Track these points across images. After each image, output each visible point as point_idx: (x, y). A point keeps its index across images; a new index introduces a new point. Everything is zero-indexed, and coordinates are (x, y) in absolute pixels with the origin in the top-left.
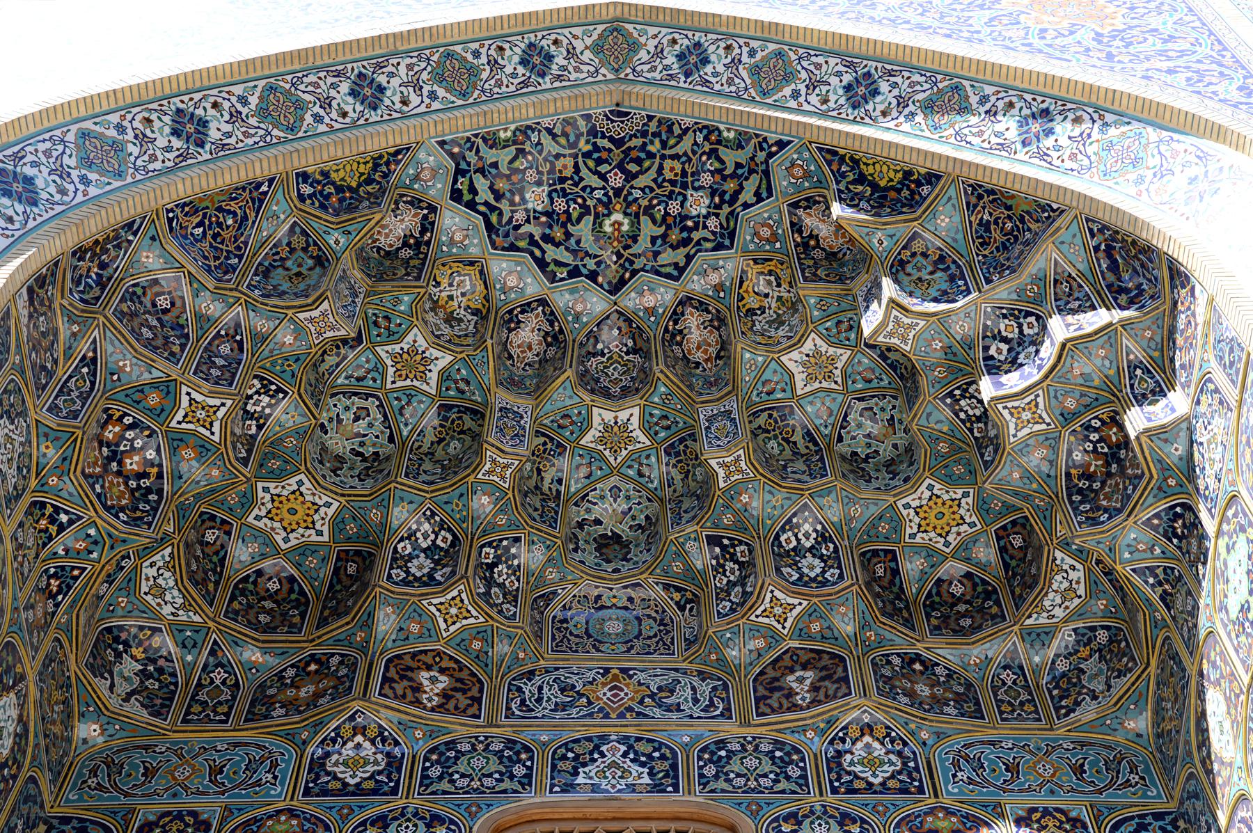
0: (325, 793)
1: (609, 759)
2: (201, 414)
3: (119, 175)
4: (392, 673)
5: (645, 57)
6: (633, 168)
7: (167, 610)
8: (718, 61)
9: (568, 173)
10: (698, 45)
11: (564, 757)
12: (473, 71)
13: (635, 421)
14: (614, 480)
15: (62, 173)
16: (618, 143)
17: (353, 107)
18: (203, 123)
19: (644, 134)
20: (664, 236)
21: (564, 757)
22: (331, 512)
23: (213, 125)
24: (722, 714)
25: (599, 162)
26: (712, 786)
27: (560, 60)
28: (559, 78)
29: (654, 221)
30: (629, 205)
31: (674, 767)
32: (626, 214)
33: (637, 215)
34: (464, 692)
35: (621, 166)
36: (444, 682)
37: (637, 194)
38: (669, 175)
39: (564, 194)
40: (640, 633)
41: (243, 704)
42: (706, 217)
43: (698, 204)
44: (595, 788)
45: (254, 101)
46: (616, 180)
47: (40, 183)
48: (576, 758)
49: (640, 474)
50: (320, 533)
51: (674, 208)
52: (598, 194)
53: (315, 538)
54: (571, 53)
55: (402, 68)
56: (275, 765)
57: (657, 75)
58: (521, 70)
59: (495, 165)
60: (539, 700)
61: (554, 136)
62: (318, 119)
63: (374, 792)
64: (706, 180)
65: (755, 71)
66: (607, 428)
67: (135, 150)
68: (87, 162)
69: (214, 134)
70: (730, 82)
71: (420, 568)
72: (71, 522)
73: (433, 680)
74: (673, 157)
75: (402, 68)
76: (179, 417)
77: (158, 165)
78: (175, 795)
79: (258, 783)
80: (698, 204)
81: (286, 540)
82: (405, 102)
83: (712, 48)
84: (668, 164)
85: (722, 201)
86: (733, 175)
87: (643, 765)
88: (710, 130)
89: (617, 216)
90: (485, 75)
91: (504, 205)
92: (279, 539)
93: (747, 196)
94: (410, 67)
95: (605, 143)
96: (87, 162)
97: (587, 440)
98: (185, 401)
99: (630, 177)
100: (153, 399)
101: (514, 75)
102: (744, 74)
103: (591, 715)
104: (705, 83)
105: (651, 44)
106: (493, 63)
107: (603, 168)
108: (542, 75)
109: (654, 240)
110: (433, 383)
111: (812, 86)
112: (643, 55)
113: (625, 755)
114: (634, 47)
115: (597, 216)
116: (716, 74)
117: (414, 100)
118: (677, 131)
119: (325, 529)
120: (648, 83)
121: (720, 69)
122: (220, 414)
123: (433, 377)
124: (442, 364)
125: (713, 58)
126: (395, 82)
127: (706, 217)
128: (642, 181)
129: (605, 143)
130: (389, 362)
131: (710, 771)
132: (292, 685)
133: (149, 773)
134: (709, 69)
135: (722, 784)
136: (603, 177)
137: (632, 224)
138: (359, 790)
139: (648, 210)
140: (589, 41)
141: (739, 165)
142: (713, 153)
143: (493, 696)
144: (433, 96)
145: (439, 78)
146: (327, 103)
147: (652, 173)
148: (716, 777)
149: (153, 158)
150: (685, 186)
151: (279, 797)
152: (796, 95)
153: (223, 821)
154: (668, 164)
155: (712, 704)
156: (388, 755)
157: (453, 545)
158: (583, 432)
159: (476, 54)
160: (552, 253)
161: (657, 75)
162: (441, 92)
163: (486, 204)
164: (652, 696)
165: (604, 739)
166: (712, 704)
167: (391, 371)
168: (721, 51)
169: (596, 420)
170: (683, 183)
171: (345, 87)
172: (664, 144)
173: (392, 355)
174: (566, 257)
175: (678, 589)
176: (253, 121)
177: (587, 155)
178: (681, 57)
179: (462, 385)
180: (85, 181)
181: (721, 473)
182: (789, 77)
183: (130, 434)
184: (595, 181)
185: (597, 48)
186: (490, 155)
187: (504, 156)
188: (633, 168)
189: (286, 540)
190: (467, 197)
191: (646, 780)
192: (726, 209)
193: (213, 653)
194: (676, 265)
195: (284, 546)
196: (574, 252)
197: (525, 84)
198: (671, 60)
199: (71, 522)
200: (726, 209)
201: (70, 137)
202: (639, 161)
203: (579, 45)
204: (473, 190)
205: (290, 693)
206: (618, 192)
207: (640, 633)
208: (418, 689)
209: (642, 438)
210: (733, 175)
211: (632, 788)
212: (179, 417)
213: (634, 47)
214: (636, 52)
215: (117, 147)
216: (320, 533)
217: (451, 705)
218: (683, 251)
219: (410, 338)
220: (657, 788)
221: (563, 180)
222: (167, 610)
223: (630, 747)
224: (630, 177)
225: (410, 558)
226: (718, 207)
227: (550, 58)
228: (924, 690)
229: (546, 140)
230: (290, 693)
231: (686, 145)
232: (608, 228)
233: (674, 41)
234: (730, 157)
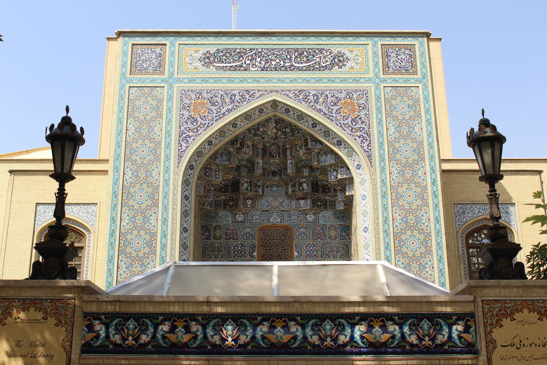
12: (251, 116)
41: (222, 204)
43: (288, 130)
51: (284, 130)
63: (243, 222)
65: (298, 116)
80: (288, 130)
93: (296, 132)
111: (307, 122)
114: (277, 106)
133: (213, 217)
138: (241, 222)
139: (280, 130)
143: (258, 204)
145: (245, 119)
152: (304, 122)
160: (264, 136)
165: (274, 212)
182: (303, 119)
185: (271, 106)
224: (277, 125)
227: (263, 110)
228: (319, 203)
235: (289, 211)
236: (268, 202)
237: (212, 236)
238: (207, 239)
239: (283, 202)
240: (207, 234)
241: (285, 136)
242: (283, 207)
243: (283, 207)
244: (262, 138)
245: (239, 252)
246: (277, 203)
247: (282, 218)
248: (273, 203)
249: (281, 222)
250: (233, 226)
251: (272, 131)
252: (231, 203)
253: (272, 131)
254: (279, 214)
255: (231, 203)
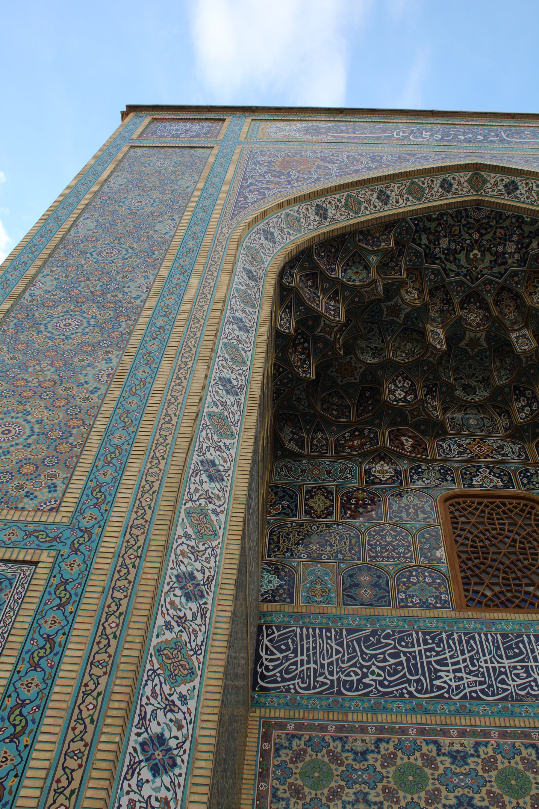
0: (374, 483)
1: (484, 475)
2: (328, 329)
3: (299, 231)
4: (392, 437)
5: (490, 186)
6: (483, 231)
7: (301, 408)
8: (522, 189)
9: (456, 233)
10: (513, 182)
11: (465, 473)
13: (483, 337)
14: (470, 361)
15: (281, 230)
16: (477, 221)
17: (378, 204)
18: (326, 210)
19: (488, 217)
20: (495, 261)
21: (465, 473)
22: (362, 370)
23: (329, 211)
24: (525, 459)
25: (469, 228)
26: (527, 486)
27: (455, 186)
28: (455, 193)
29: (491, 254)
30: (481, 247)
31: (510, 478)
32: (479, 251)
33: (484, 252)
34: (420, 446)
35: (478, 231)
36: (411, 442)
37: (485, 242)
38: (498, 235)
39: (454, 241)
40: (484, 425)
42: (514, 253)
43: (511, 248)
44: (481, 486)
45: (343, 201)
46: (476, 236)
47: (275, 235)
48: (470, 474)
49: (482, 359)
50: (356, 379)
51: (500, 249)
52: (468, 242)
53: (353, 381)
54: (459, 183)
55: (396, 188)
56: (351, 471)
57: (495, 193)
58: (440, 190)
59: (429, 229)
60: (450, 450)
61: (452, 217)
62: (366, 209)
64: (515, 238)
66: (471, 339)
67: (304, 221)
68: (289, 226)
69: (330, 215)
70: (528, 198)
71: (400, 395)
72: (283, 371)
73: (407, 441)
74: (501, 228)
75: (396, 188)
76: (319, 330)
77: (311, 227)
78: (316, 480)
79: (346, 478)
81: (342, 381)
82: (397, 202)
83: (519, 183)
84: (498, 230)
85: (522, 247)
86: (528, 237)
87: (498, 477)
88: (518, 218)
89: (475, 252)
90: (427, 191)
91: (432, 246)
92: (339, 381)
94: (399, 188)
95: (472, 221)
96: (289, 226)
97: (462, 344)
98: (322, 324)
99: (482, 235)
100: (310, 323)
101: (438, 192)
102: (534, 195)
103: (473, 457)
104: (517, 198)
105: (492, 181)
106: (430, 187)
107: (470, 231)
108: (448, 192)
109: (491, 262)
110: (402, 318)
112: (489, 185)
113: (490, 473)
114: (485, 181)
115: (467, 251)
116: (521, 194)
117: (401, 201)
118: (503, 217)
119: (358, 378)
120: (491, 197)
121: (523, 192)
122: (335, 330)
123: (402, 316)
124: (407, 311)
125: (520, 187)
126: (394, 194)
127: (514, 253)
128: (487, 237)
129: (472, 221)
130: (385, 309)
131: (525, 481)
132: (350, 440)
133: (303, 471)
134: (518, 192)
135: (531, 486)
136: (470, 235)
137: (481, 255)
139: (489, 250)
140: (466, 179)
141: (531, 232)
142: (519, 227)
143: (432, 448)
144: (407, 199)
146: (369, 202)
147: (491, 234)
148: (528, 483)
149: (310, 224)
150: (505, 240)
151: (356, 482)
153: (337, 491)
154: (498, 230)
155: (520, 454)
156: (395, 470)
157: (411, 386)
158: (461, 341)
159: (423, 183)
160: (449, 266)
161: (495, 193)
162: (410, 198)
163: (425, 245)
164: (495, 450)
165: (480, 467)
166: (520, 454)
167: (385, 313)
168: (524, 185)
169: (467, 336)
170: (505, 239)
171: (375, 196)
172: (497, 222)
173: (387, 307)
174: (454, 268)
175: (498, 407)
176: (343, 209)
177: (464, 226)
178: (505, 186)
179: (414, 320)
180: (289, 234)
181: (524, 360)
183: (299, 337)
184: (467, 237)
186: (428, 224)
187: (433, 225)
188: (483, 231)
189: (342, 381)
190: (418, 242)
191: (501, 483)
192: (524, 250)
193: (317, 425)
194: (500, 273)
195: (340, 383)
196: (458, 266)
197: (442, 195)
198: (501, 187)
199: (283, 371)
200: (524, 250)
201: (283, 216)
202: (486, 229)
203: (462, 180)
204: (421, 239)
205: (350, 443)
206: (476, 241)
207: (484, 425)
208: (402, 444)
209: (485, 345)
210: (528, 237)
211: (495, 486)
212: (319, 330)
213: (485, 181)
214: (486, 183)
215: (298, 220)
216: (356, 379)
217: (416, 450)
218: (503, 267)
219: (395, 300)
220: (506, 486)
221: (454, 236)
222: (301, 408)
223: (491, 471)
224: (482, 235)
225: (395, 391)
226: (520, 249)
229: (450, 219)
230: (350, 443)
231: (507, 223)
232: (472, 257)
233: (502, 180)
234: (527, 229)
235: (524, 464)
236: (460, 446)
237: (302, 508)
238: (287, 515)
239: (502, 447)
240: (285, 503)
241: (502, 269)
242: (507, 455)
243: (507, 455)
244: (444, 269)
245: (390, 548)
246: (485, 449)
247: (506, 478)
248: (476, 449)
249: (506, 486)
250: (363, 490)
251: (468, 255)
252: (357, 443)
253: (468, 255)
254: (496, 471)
255: (357, 443)
